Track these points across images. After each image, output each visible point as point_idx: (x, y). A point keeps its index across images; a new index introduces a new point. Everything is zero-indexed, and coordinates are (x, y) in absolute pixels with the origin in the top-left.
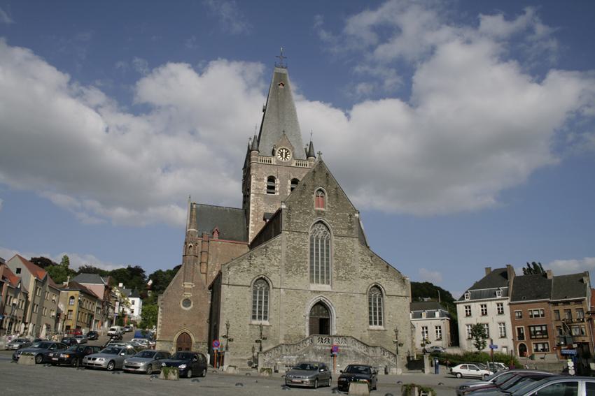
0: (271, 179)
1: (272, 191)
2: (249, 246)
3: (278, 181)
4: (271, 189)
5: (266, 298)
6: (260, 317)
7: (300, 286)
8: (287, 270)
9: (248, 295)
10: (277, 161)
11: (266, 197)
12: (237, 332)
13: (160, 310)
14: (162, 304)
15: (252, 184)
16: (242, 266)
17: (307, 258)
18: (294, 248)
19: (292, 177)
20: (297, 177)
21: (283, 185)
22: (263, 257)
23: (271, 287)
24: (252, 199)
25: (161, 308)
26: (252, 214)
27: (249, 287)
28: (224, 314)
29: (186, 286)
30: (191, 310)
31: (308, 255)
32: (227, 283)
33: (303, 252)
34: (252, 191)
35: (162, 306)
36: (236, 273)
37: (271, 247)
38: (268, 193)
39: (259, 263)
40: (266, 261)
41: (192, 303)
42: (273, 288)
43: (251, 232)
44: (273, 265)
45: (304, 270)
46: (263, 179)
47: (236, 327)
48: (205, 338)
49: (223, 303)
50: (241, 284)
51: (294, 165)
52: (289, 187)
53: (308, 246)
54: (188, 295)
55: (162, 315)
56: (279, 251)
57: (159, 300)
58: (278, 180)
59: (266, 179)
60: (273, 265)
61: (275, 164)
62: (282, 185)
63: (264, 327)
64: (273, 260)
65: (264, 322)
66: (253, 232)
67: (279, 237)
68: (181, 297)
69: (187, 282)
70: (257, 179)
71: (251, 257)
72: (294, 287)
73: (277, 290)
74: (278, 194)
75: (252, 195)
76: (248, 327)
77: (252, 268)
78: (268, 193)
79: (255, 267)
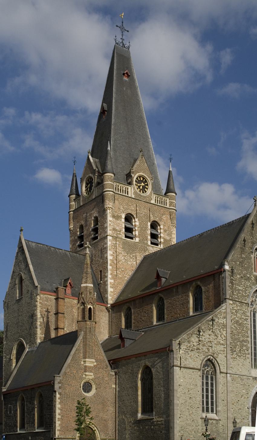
0: (129, 218)
1: (129, 234)
2: (107, 308)
3: (136, 222)
4: (129, 230)
5: (212, 384)
6: (207, 411)
7: (245, 372)
8: (233, 351)
9: (197, 378)
10: (135, 193)
11: (124, 243)
12: (191, 428)
13: (58, 396)
14: (60, 388)
15: (109, 223)
16: (191, 343)
17: (248, 337)
18: (237, 322)
19: (152, 219)
20: (157, 219)
21: (143, 229)
22: (210, 332)
23: (218, 371)
24: (109, 243)
25: (60, 394)
26: (111, 265)
27: (199, 370)
28: (178, 405)
29: (87, 364)
30: (94, 396)
31: (249, 332)
32: (179, 364)
33: (245, 329)
34: (109, 232)
35: (60, 391)
36: (186, 352)
37: (217, 320)
38: (126, 237)
39: (207, 340)
40: (213, 336)
41: (94, 387)
42: (221, 372)
43: (110, 290)
44: (219, 343)
45: (246, 351)
46: (121, 217)
47: (189, 422)
48: (110, 433)
49: (177, 391)
50: (191, 366)
51: (153, 202)
52: (149, 232)
53: (249, 320)
54: (90, 376)
55: (60, 403)
56: (225, 326)
57: (56, 382)
58: (137, 220)
59: (123, 216)
60: (219, 343)
61: (133, 196)
62: (142, 228)
63: (210, 421)
64: (219, 338)
65: (210, 415)
66: (112, 290)
67: (224, 307)
68: (81, 378)
69: (89, 358)
70: (113, 216)
71: (199, 331)
72: (238, 373)
73: (224, 375)
74: (137, 240)
75: (109, 238)
76: (200, 420)
77: (201, 347)
78: (126, 237)
79: (204, 345)
